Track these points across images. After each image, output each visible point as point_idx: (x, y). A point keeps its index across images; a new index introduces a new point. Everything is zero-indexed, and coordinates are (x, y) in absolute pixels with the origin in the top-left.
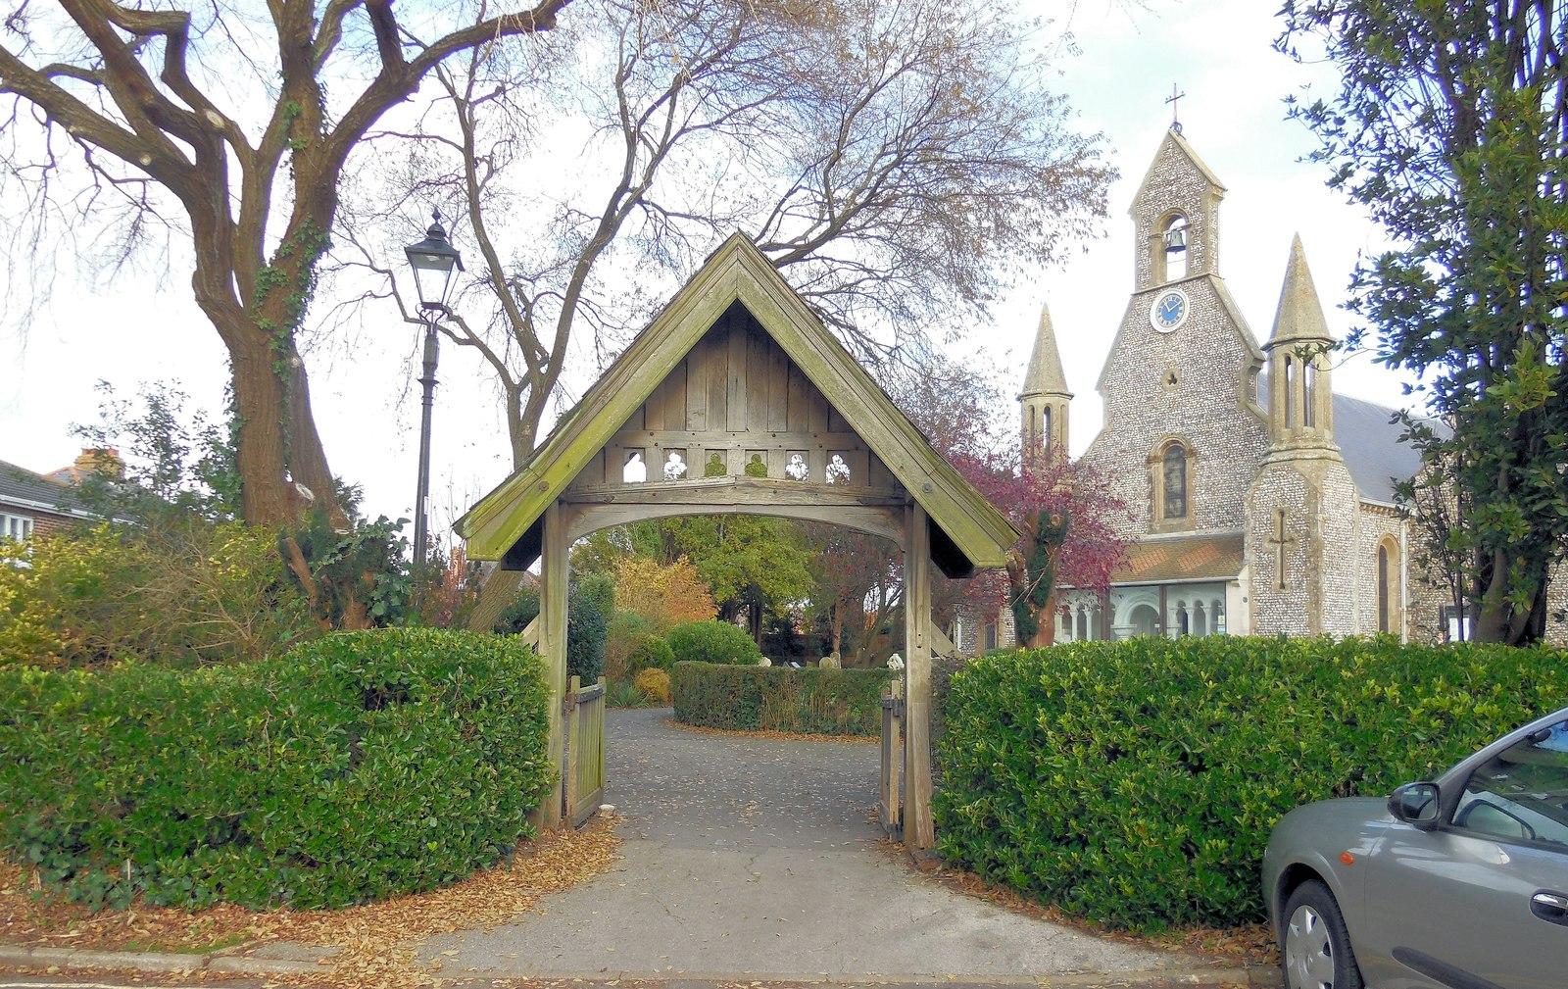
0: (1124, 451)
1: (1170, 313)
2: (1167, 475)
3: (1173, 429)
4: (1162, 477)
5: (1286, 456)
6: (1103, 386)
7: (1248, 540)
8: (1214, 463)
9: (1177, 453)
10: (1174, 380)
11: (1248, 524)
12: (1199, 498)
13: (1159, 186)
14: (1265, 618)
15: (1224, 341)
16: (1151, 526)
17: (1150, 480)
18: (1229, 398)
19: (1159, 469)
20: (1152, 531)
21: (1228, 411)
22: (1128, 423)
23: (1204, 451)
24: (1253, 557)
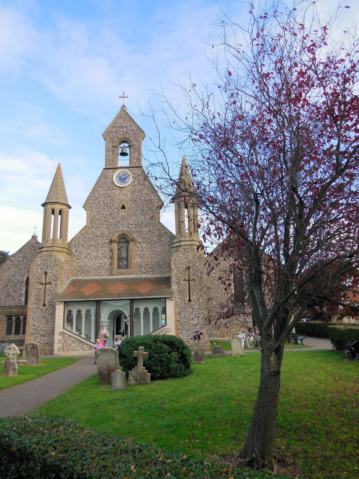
0: (98, 236)
1: (122, 179)
2: (119, 249)
4: (116, 250)
5: (189, 243)
7: (174, 279)
8: (144, 245)
9: (125, 240)
10: (123, 207)
12: (136, 260)
13: (117, 127)
14: (182, 315)
16: (111, 272)
17: (111, 251)
19: (115, 246)
20: (112, 274)
23: (139, 240)
24: (176, 287)
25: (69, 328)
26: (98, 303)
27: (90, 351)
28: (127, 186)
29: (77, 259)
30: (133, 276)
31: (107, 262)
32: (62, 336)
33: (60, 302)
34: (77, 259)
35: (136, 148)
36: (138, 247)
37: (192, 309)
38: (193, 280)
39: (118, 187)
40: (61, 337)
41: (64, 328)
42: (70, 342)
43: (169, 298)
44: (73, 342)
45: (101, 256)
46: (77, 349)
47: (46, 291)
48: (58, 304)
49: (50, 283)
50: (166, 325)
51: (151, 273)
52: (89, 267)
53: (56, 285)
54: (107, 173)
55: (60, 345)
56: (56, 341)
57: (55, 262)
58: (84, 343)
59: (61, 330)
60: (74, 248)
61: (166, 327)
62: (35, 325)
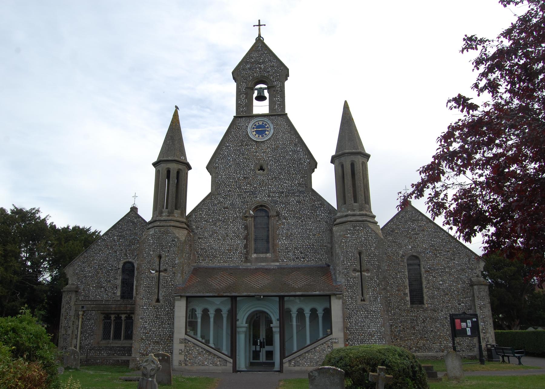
0: (227, 208)
3: (261, 198)
6: (210, 167)
8: (291, 221)
10: (261, 169)
11: (339, 259)
13: (252, 63)
14: (353, 320)
15: (295, 152)
17: (246, 228)
18: (300, 184)
20: (247, 260)
21: (300, 192)
22: (230, 191)
23: (284, 213)
24: (343, 280)
25: (192, 333)
26: (234, 299)
27: (224, 367)
28: (266, 140)
29: (199, 238)
30: (278, 264)
31: (240, 243)
32: (183, 345)
33: (181, 296)
34: (199, 238)
35: (277, 90)
36: (283, 224)
37: (367, 311)
38: (367, 270)
39: (254, 141)
40: (182, 346)
41: (186, 334)
42: (195, 353)
43: (335, 295)
44: (199, 354)
45: (232, 235)
46: (206, 363)
47: (161, 281)
48: (178, 300)
49: (165, 270)
50: (331, 333)
51: (302, 260)
52: (216, 250)
53: (174, 273)
54: (238, 123)
55: (182, 358)
56: (176, 351)
57: (173, 241)
58: (215, 355)
59: (183, 336)
60: (194, 223)
61: (330, 337)
62: (145, 328)
